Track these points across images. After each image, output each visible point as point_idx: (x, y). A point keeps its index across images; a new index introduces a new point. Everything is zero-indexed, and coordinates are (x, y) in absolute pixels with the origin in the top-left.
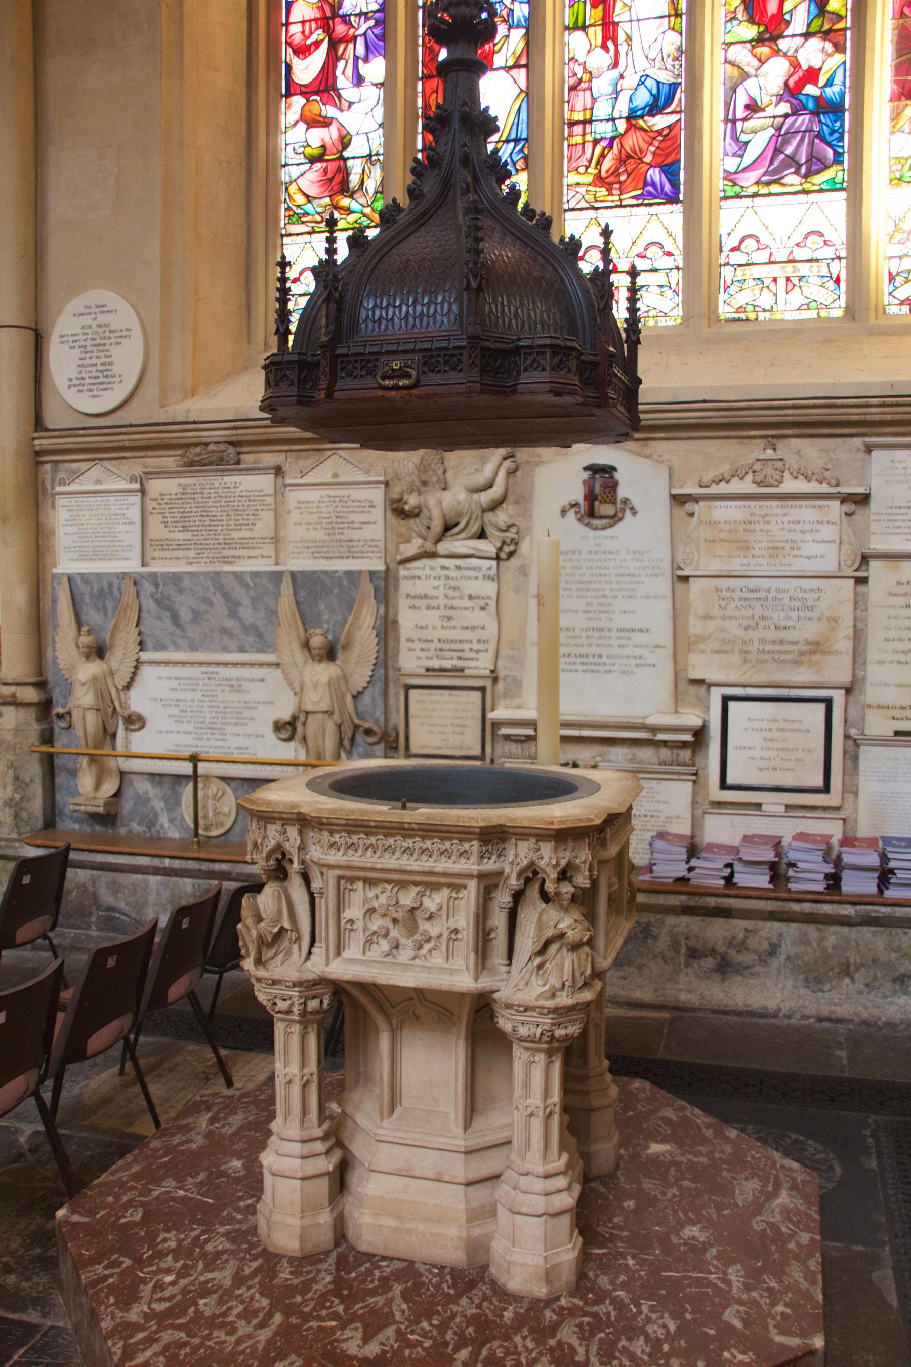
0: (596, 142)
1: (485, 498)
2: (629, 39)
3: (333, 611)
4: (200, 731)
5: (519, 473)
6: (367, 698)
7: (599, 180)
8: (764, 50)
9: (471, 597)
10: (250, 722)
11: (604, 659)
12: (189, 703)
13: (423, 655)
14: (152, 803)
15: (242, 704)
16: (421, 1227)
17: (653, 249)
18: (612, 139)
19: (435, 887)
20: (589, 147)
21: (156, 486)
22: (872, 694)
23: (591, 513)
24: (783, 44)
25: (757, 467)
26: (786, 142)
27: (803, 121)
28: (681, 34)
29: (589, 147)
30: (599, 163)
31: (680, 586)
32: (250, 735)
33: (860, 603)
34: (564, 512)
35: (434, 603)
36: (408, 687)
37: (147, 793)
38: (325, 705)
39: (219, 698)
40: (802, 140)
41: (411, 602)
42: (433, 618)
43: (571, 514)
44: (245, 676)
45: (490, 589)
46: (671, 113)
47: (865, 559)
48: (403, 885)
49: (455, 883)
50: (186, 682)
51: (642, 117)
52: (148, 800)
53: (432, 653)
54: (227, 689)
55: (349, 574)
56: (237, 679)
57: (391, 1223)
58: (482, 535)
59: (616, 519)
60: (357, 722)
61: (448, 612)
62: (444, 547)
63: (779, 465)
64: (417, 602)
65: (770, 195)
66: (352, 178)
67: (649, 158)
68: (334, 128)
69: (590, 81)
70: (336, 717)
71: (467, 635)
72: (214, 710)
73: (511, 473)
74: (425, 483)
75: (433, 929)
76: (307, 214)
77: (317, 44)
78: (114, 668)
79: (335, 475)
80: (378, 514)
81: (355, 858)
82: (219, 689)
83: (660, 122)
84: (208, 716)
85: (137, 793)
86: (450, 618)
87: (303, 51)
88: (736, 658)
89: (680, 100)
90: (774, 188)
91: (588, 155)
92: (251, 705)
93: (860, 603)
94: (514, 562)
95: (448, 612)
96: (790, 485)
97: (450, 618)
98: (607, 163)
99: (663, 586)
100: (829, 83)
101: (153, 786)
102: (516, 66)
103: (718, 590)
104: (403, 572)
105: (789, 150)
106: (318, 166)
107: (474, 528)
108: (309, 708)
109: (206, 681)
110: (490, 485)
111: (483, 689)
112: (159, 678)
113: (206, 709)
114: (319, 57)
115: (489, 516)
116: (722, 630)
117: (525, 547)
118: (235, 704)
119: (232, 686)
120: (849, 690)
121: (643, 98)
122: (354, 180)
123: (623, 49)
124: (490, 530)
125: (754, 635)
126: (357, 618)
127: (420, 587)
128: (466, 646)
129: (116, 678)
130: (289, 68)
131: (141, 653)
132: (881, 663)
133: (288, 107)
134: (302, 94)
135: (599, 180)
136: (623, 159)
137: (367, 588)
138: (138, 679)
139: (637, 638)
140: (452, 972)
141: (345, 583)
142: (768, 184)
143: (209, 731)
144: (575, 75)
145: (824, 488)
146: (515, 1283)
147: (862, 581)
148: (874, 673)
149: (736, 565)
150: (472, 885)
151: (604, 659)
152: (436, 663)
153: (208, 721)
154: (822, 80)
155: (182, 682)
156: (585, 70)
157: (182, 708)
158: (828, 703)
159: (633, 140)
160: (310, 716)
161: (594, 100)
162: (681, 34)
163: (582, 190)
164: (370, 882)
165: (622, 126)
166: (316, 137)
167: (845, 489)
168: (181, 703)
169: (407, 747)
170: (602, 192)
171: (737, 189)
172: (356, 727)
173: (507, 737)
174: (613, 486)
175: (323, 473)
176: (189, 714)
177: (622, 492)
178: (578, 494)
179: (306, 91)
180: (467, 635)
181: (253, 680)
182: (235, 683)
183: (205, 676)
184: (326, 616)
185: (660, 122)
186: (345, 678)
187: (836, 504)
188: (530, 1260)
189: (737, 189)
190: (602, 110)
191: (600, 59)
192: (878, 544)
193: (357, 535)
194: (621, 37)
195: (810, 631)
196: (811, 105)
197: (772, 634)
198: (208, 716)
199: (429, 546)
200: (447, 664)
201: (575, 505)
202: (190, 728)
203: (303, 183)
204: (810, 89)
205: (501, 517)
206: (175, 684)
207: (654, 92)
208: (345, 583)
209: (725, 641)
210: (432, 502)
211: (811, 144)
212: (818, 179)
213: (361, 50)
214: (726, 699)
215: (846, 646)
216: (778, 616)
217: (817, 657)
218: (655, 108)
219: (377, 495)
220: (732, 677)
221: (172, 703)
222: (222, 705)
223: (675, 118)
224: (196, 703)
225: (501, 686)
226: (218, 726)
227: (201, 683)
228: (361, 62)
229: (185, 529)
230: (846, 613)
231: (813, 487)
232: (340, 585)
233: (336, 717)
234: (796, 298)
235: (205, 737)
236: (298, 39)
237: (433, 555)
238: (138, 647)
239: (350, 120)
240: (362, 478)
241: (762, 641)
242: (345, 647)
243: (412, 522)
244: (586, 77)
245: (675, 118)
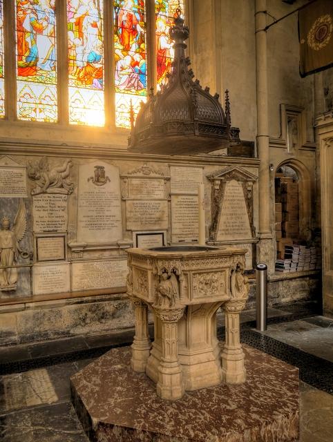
1: (63, 174)
2: (87, 38)
3: (8, 212)
5: (73, 167)
6: (22, 242)
8: (125, 53)
9: (59, 207)
11: (102, 225)
13: (42, 226)
16: (207, 376)
17: (95, 103)
19: (216, 272)
20: (75, 68)
22: (174, 231)
23: (98, 181)
24: (130, 53)
25: (144, 169)
26: (131, 80)
27: (135, 75)
29: (75, 68)
30: (79, 74)
31: (123, 203)
33: (170, 207)
34: (88, 180)
35: (46, 209)
36: (37, 238)
38: (10, 246)
41: (37, 209)
42: (45, 214)
43: (91, 181)
45: (65, 204)
47: (170, 195)
48: (208, 273)
49: (222, 270)
53: (45, 226)
55: (14, 199)
57: (199, 378)
58: (62, 186)
59: (104, 183)
60: (21, 251)
61: (51, 212)
62: (49, 190)
64: (40, 209)
67: (94, 76)
70: (14, 250)
71: (58, 219)
73: (71, 167)
74: (42, 169)
75: (216, 285)
79: (6, 164)
80: (25, 178)
81: (199, 267)
86: (52, 214)
88: (139, 223)
90: (129, 92)
93: (170, 207)
94: (72, 195)
95: (51, 212)
96: (152, 175)
97: (52, 214)
98: (81, 74)
99: (118, 203)
102: (51, 36)
103: (133, 204)
104: (34, 198)
105: (132, 82)
107: (59, 184)
108: (4, 247)
110: (65, 171)
111: (64, 237)
115: (64, 180)
116: (135, 215)
117: (76, 191)
120: (167, 230)
121: (92, 58)
123: (85, 41)
124: (64, 185)
125: (144, 216)
126: (19, 214)
127: (42, 203)
128: (58, 223)
132: (175, 223)
135: (79, 79)
136: (86, 74)
137: (23, 203)
139: (111, 218)
140: (223, 295)
141: (13, 202)
142: (127, 90)
145: (160, 176)
146: (238, 382)
147: (169, 201)
148: (174, 226)
149: (139, 197)
150: (228, 272)
151: (102, 225)
152: (47, 229)
154: (140, 66)
158: (163, 234)
159: (89, 69)
164: (200, 274)
169: (37, 259)
170: (80, 83)
172: (20, 252)
173: (74, 251)
174: (103, 173)
177: (106, 175)
178: (93, 175)
180: (58, 219)
184: (5, 214)
186: (15, 235)
187: (163, 180)
188: (241, 373)
191: (78, 42)
192: (173, 191)
193: (16, 185)
194: (84, 37)
195: (158, 215)
196: (138, 72)
197: (148, 216)
199: (44, 189)
200: (51, 229)
201: (92, 178)
205: (68, 181)
208: (13, 202)
209: (136, 219)
210: (45, 175)
211: (138, 82)
212: (140, 92)
214: (137, 235)
215: (166, 218)
216: (149, 211)
217: (160, 222)
218: (95, 61)
219: (24, 172)
220: (139, 229)
225: (69, 235)
230: (166, 210)
231: (157, 175)
232: (11, 203)
233: (14, 250)
237: (44, 193)
240: (17, 165)
241: (146, 218)
242: (15, 225)
243: (37, 182)
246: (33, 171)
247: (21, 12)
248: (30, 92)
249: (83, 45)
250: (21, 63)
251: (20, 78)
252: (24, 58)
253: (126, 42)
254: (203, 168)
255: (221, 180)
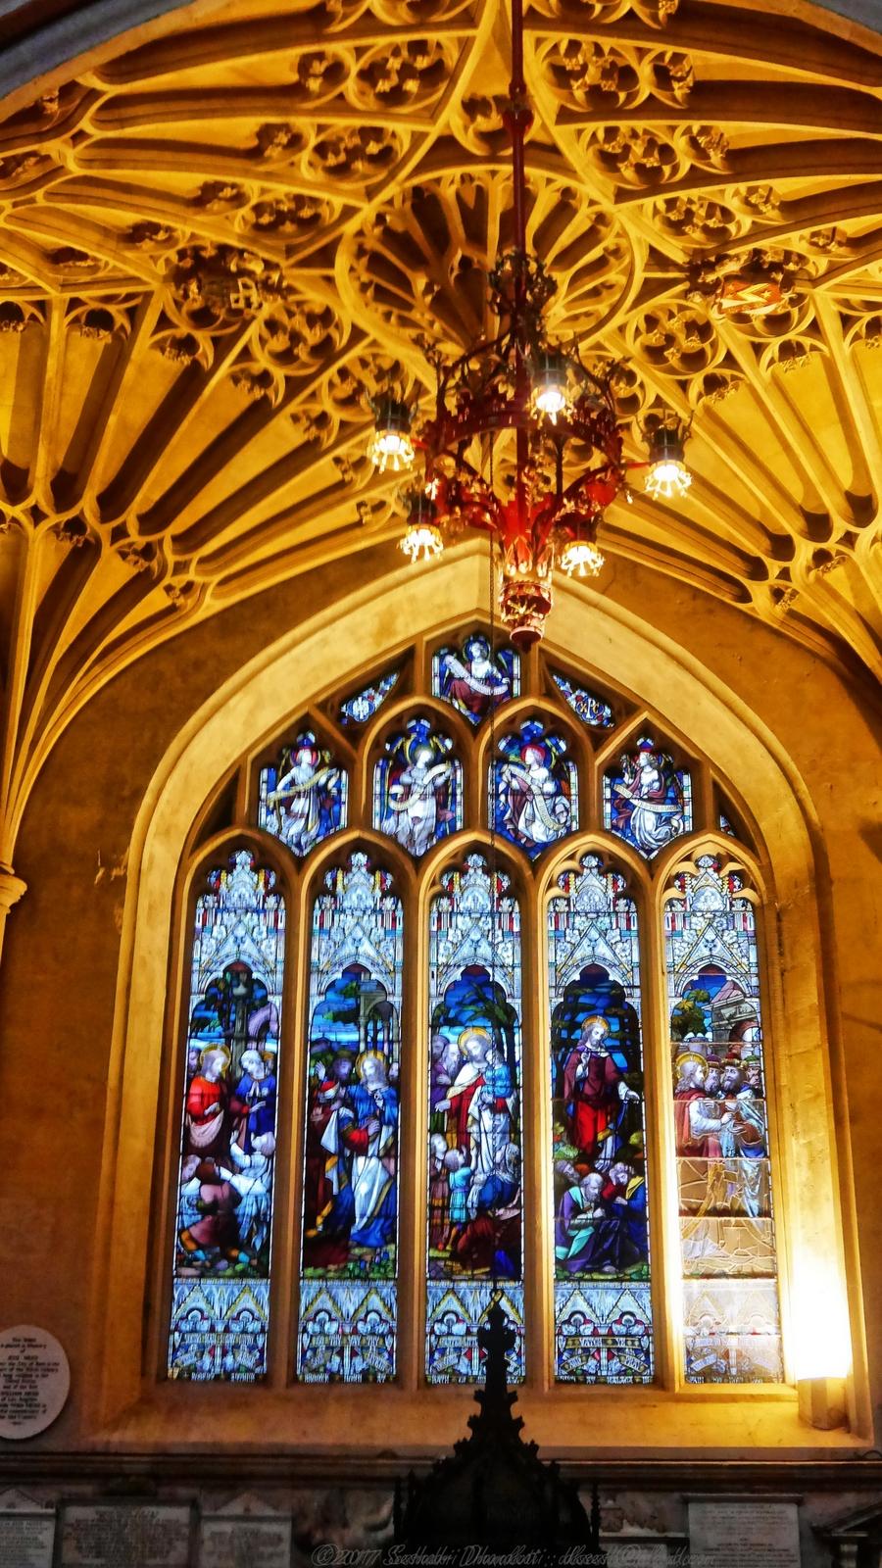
0: (452, 1225)
2: (479, 1145)
7: (454, 1257)
18: (465, 1225)
21: (75, 1513)
27: (616, 1222)
28: (520, 1147)
40: (616, 1236)
46: (514, 1207)
51: (490, 1208)
63: (619, 1513)
65: (592, 1280)
66: (241, 1232)
68: (226, 1188)
69: (448, 1174)
76: (197, 1259)
77: (214, 1115)
80: (286, 1547)
83: (505, 1214)
87: (202, 1119)
89: (520, 1198)
91: (446, 1233)
96: (631, 1531)
98: (461, 1243)
100: (634, 1197)
106: (209, 1218)
114: (213, 1127)
121: (489, 1194)
122: (244, 1233)
123: (473, 1153)
130: (188, 1130)
133: (185, 1164)
134: (199, 1154)
135: (454, 1257)
142: (590, 1271)
144: (435, 1168)
145: (653, 1534)
156: (443, 1165)
159: (482, 1226)
161: (451, 1191)
162: (520, 1147)
163: (442, 1264)
165: (473, 1215)
166: (208, 1193)
167: (671, 1535)
170: (457, 1266)
171: (567, 1273)
175: (236, 1508)
179: (202, 1152)
185: (505, 1214)
189: (567, 1273)
190: (458, 1199)
194: (472, 1144)
203: (195, 1231)
204: (620, 1200)
207: (500, 1188)
213: (253, 1124)
219: (284, 1530)
223: (516, 1212)
228: (252, 1136)
229: (98, 1555)
234: (615, 1365)
236: (196, 1109)
239: (242, 1183)
244: (444, 1171)
245: (516, 1212)
246: (305, 1527)
247: (319, 1111)
248: (329, 1305)
249: (467, 1163)
250: (312, 1233)
251: (310, 1271)
252: (319, 1220)
253: (588, 1138)
254: (799, 1503)
255: (859, 1541)
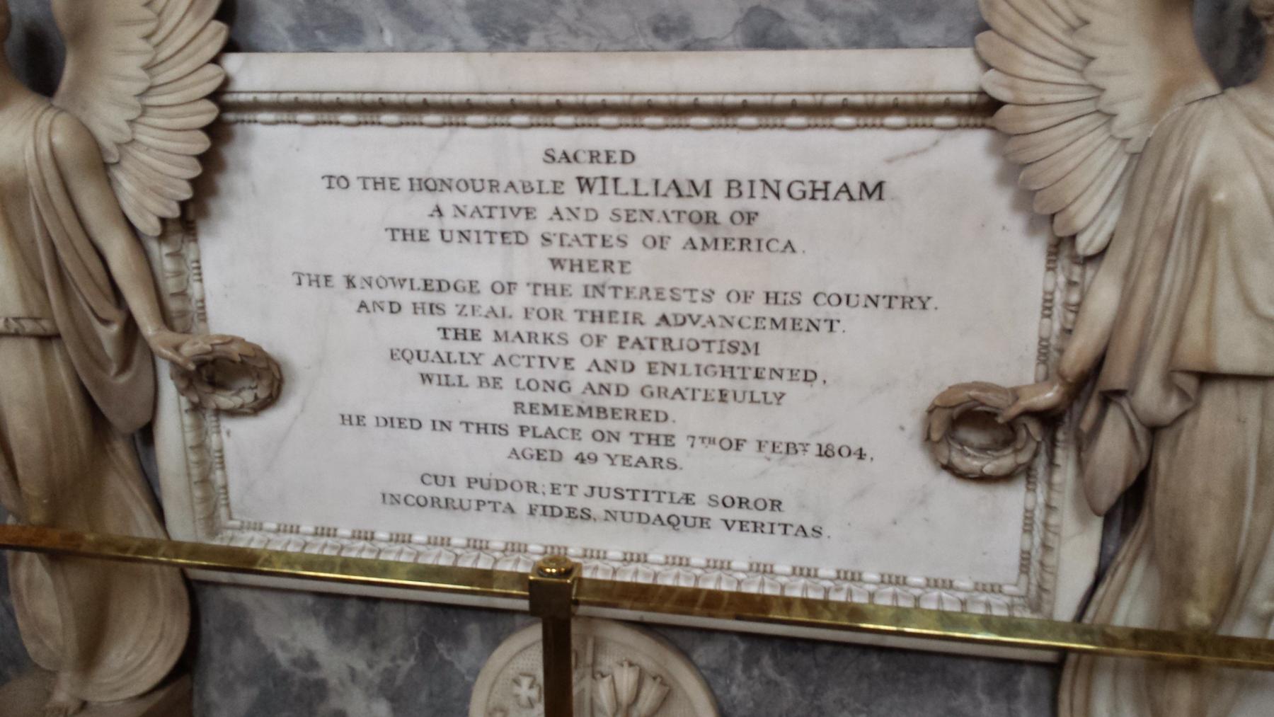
4: (542, 423)
10: (795, 391)
12: (486, 300)
14: (334, 703)
15: (757, 307)
32: (791, 448)
37: (311, 662)
39: (637, 278)
44: (783, 173)
50: (469, 199)
52: (320, 689)
54: (681, 233)
56: (733, 187)
72: (612, 332)
78: (106, 136)
82: (636, 232)
84: (583, 357)
85: (269, 663)
92: (805, 311)
101: (336, 639)
109: (572, 197)
112: (336, 181)
113: (573, 328)
118: (719, 307)
119: (709, 219)
129: (127, 186)
131: (233, 62)
138: (232, 182)
143: (587, 425)
153: (580, 378)
155: (447, 200)
157: (452, 320)
160: (1216, 400)
168: (450, 300)
176: (489, 348)
181: (819, 191)
182: (720, 204)
183: (568, 173)
198: (583, 357)
202: (497, 406)
206: (415, 210)
221: (406, 297)
222: (651, 310)
224: (523, 297)
226: (634, 401)
227: (544, 204)
235: (569, 448)
238: (217, 34)
